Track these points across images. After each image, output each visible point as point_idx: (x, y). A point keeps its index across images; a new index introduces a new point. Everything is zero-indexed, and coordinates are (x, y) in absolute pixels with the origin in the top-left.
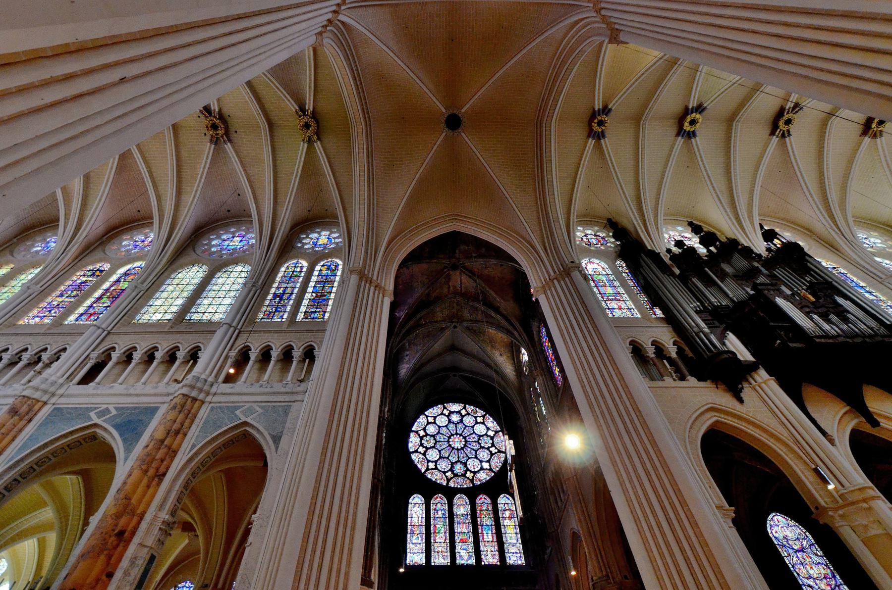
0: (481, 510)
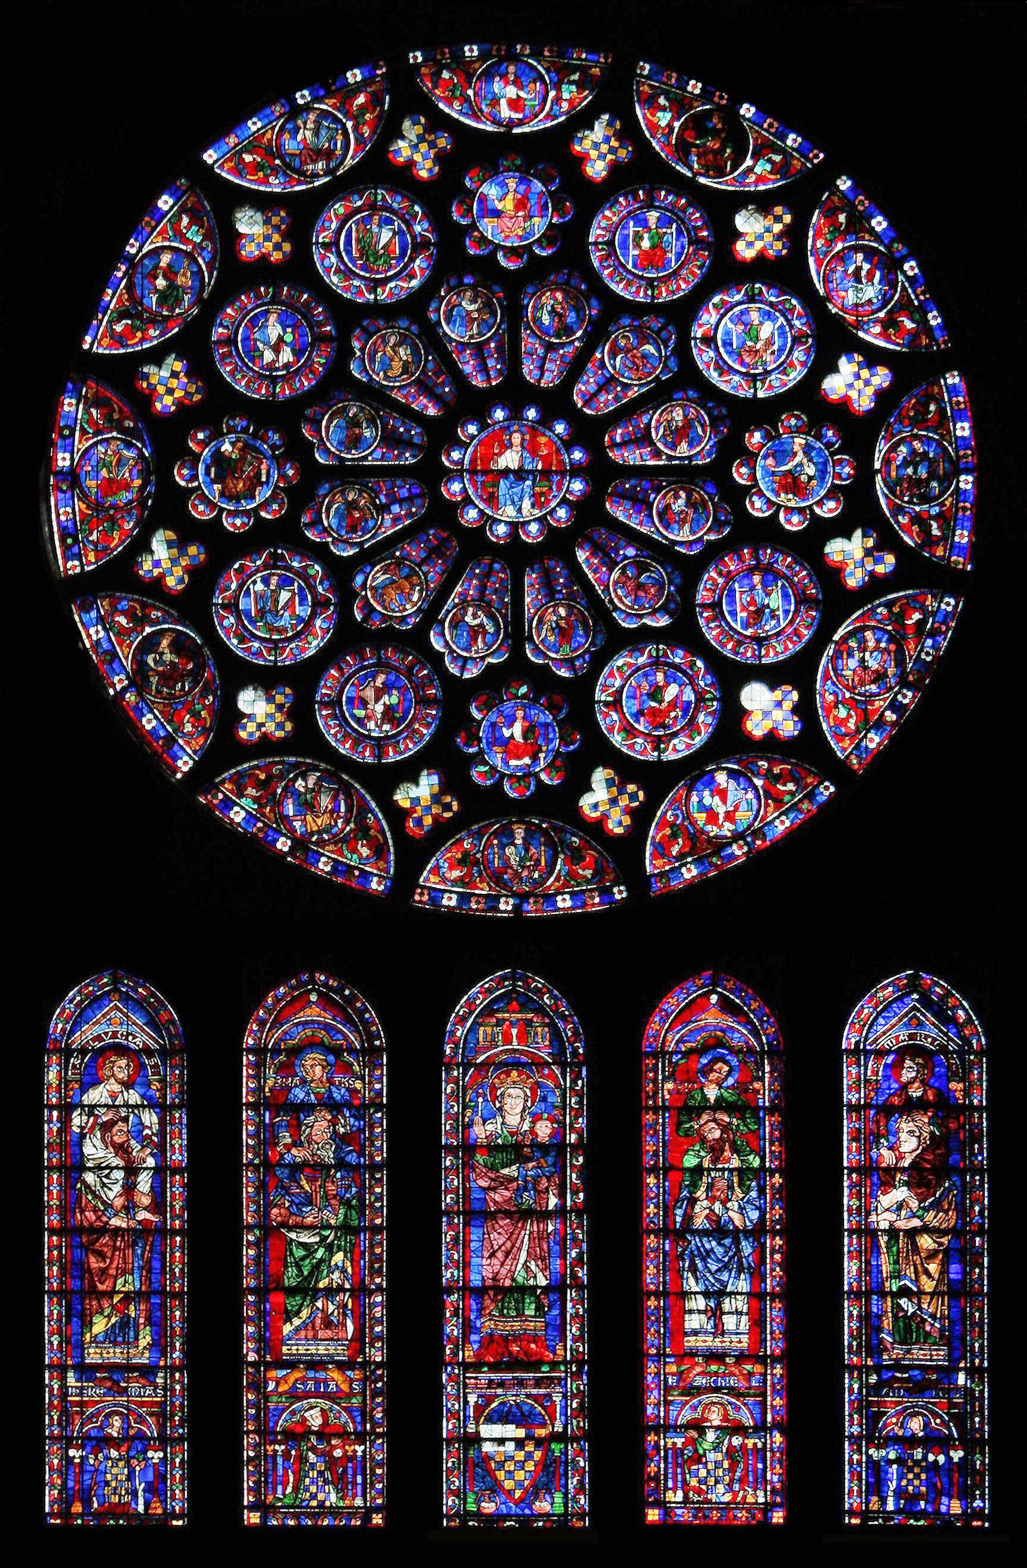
0: (688, 1109)
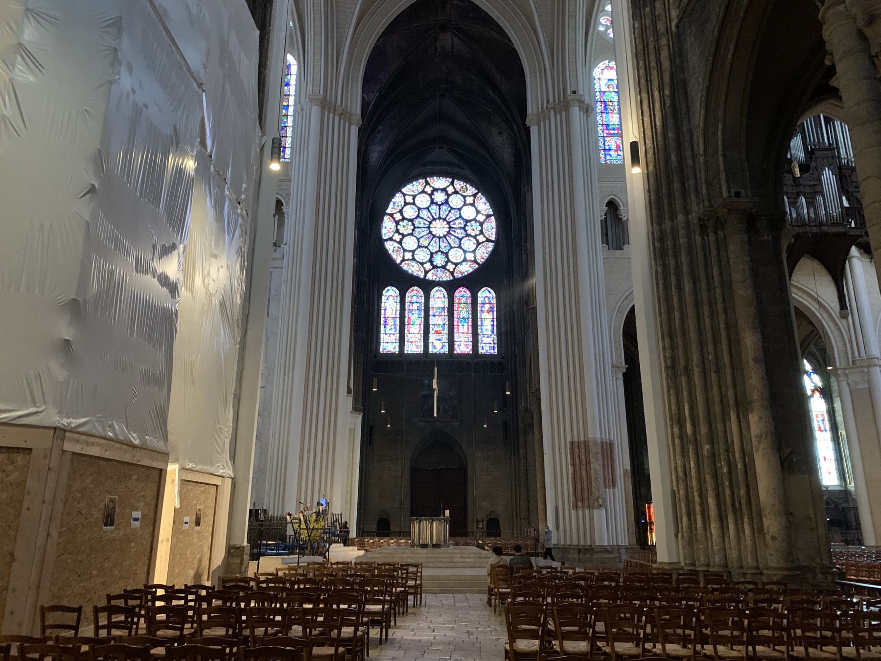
0: (459, 303)
